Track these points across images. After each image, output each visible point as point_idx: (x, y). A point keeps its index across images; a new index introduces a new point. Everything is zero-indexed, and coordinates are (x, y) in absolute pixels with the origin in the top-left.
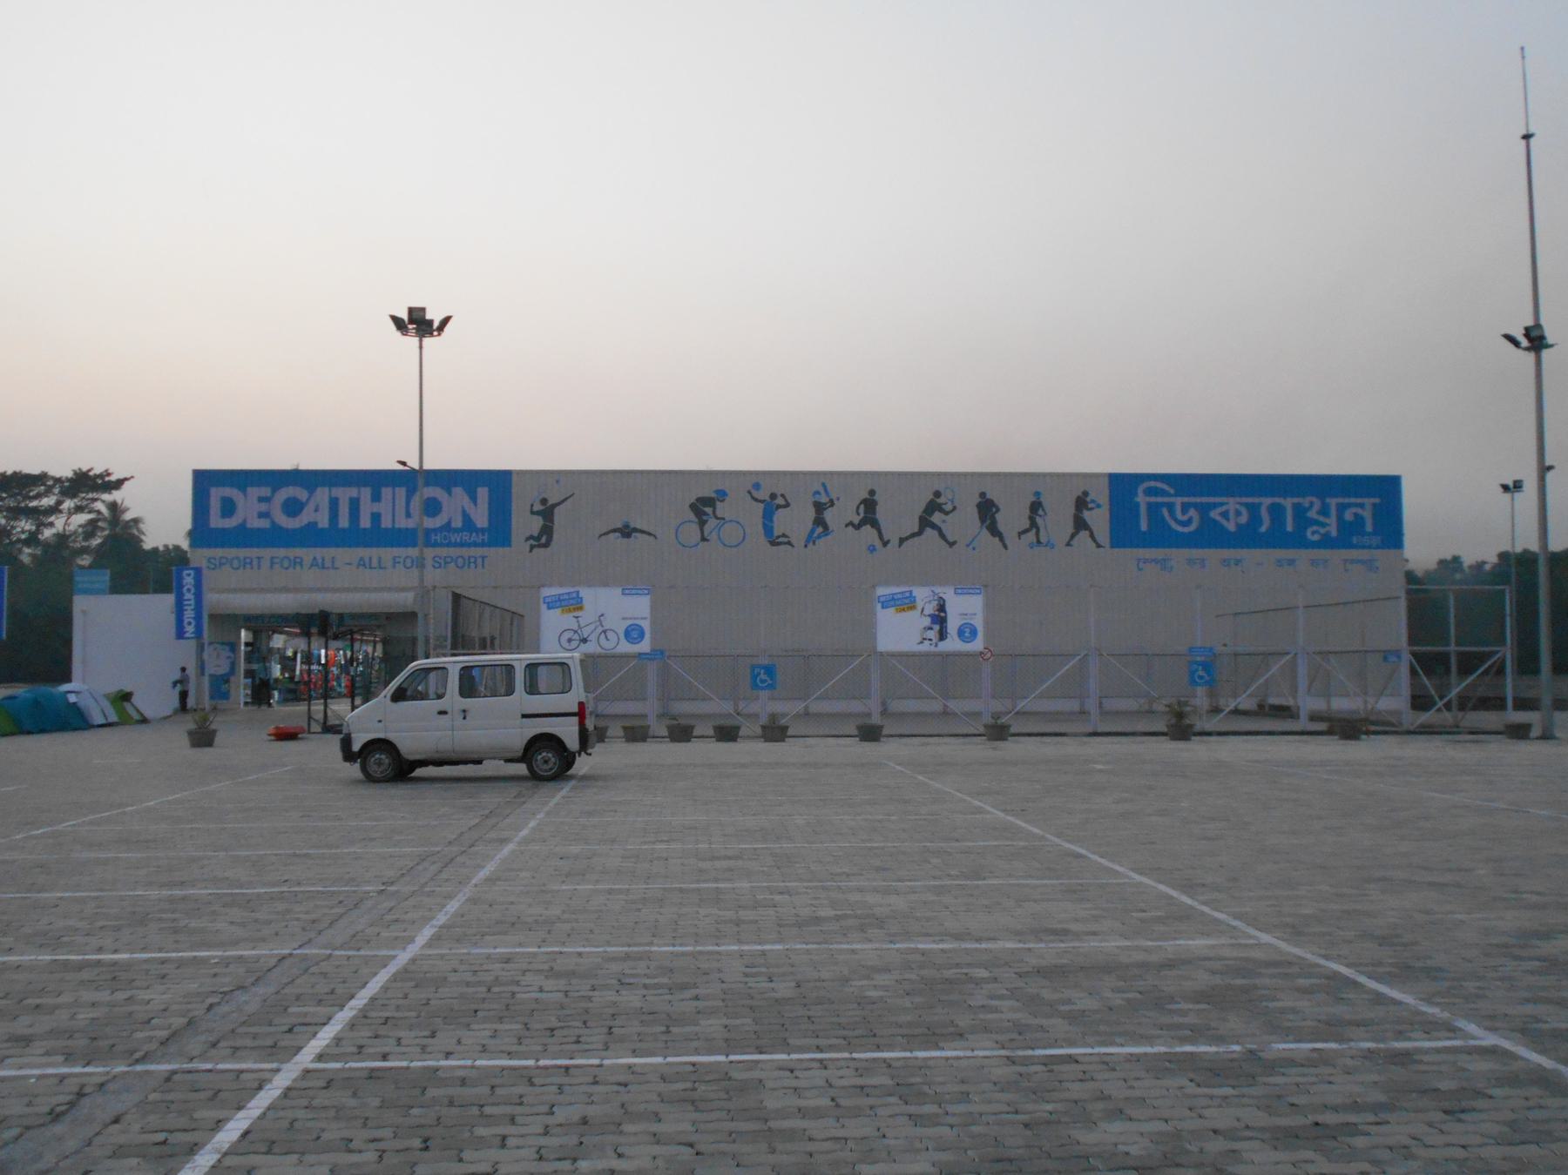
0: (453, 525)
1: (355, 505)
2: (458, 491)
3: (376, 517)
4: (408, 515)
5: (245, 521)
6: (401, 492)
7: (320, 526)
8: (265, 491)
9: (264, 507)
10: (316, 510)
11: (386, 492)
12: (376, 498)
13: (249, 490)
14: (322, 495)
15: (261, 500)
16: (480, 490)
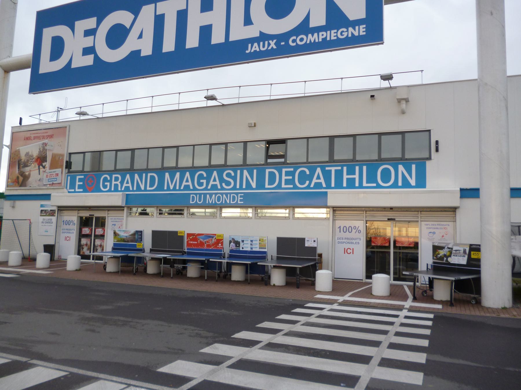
0: (313, 24)
4: (248, 21)
8: (90, 23)
9: (88, 42)
10: (140, 37)
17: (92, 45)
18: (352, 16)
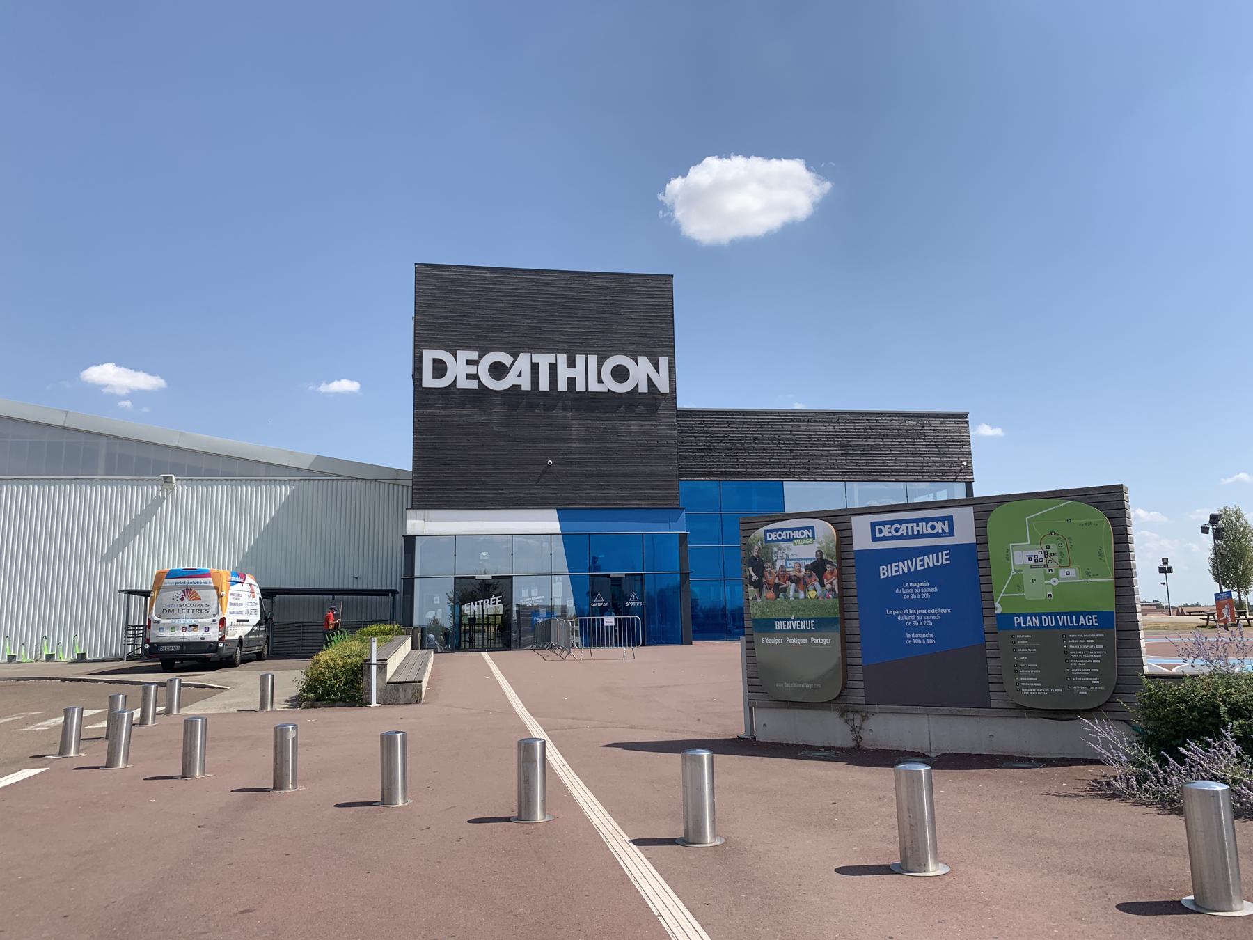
1: (553, 368)
2: (643, 360)
3: (571, 382)
4: (600, 381)
5: (455, 381)
6: (593, 359)
7: (523, 389)
8: (474, 355)
9: (472, 370)
10: (520, 375)
11: (580, 359)
12: (571, 364)
14: (524, 361)
15: (469, 362)
17: (476, 373)
18: (662, 392)
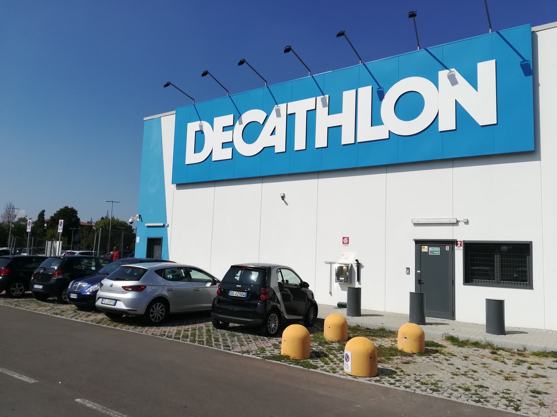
8: (228, 120)
13: (216, 120)
15: (225, 129)
16: (481, 66)
